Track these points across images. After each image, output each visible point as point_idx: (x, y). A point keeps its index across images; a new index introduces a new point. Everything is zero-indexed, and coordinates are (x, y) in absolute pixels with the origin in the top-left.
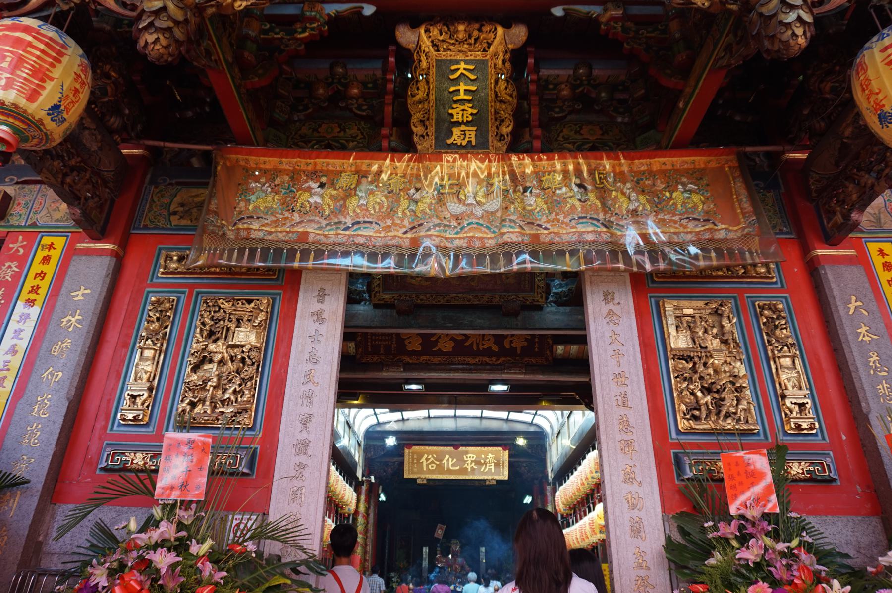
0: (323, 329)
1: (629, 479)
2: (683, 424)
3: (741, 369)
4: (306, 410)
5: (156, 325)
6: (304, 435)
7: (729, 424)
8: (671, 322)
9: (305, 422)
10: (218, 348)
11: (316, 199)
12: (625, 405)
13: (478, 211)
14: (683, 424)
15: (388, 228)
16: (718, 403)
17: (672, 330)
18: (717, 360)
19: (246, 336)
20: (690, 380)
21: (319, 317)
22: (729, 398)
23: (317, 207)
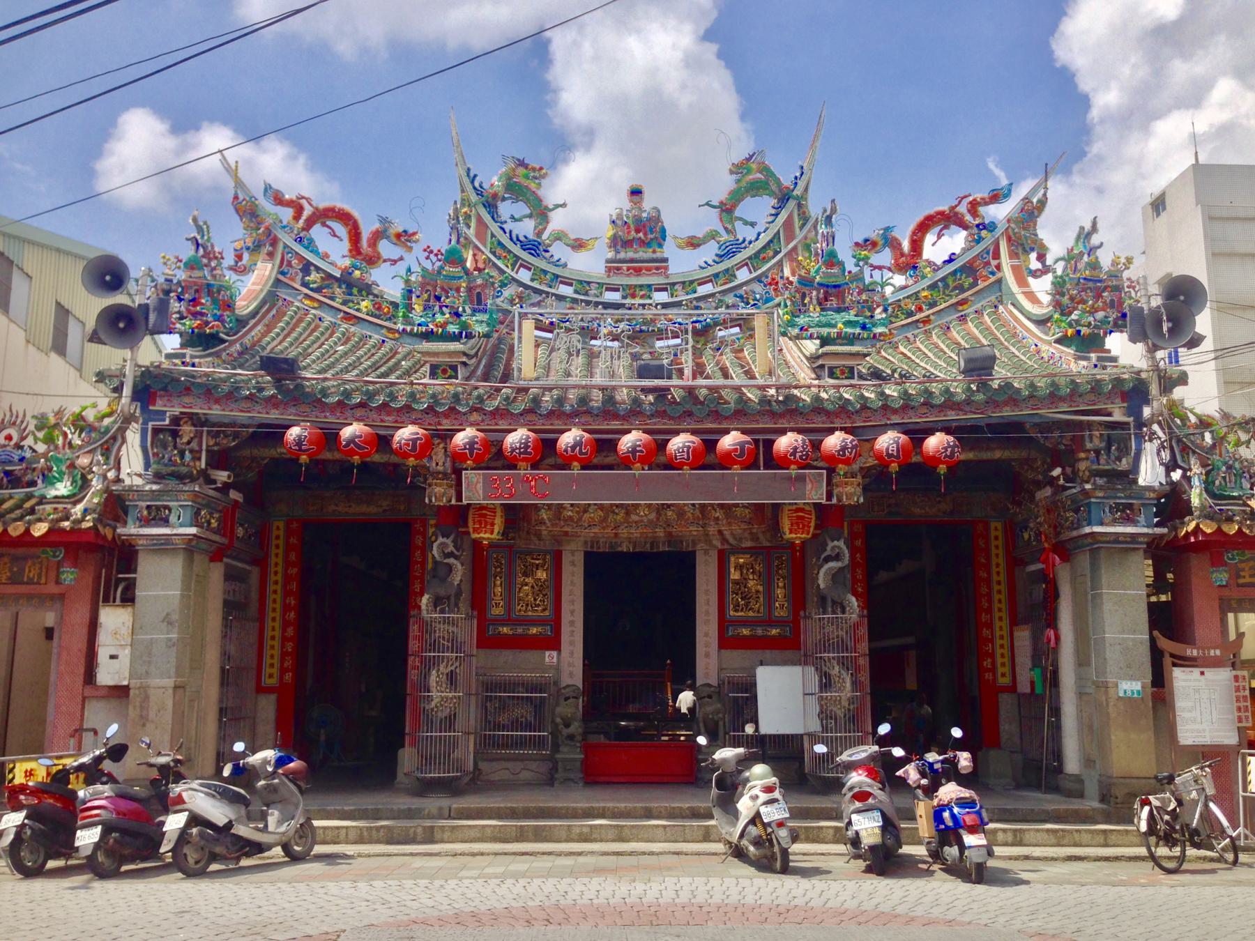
0: (575, 569)
1: (706, 635)
2: (732, 613)
3: (760, 588)
4: (572, 607)
5: (499, 570)
6: (572, 618)
7: (751, 614)
8: (732, 565)
9: (572, 612)
10: (530, 580)
11: (570, 513)
12: (708, 604)
13: (645, 519)
14: (732, 613)
15: (604, 528)
16: (747, 605)
17: (732, 570)
18: (751, 584)
19: (542, 575)
20: (737, 594)
21: (573, 563)
22: (753, 602)
23: (570, 517)
